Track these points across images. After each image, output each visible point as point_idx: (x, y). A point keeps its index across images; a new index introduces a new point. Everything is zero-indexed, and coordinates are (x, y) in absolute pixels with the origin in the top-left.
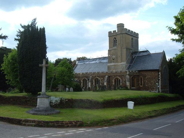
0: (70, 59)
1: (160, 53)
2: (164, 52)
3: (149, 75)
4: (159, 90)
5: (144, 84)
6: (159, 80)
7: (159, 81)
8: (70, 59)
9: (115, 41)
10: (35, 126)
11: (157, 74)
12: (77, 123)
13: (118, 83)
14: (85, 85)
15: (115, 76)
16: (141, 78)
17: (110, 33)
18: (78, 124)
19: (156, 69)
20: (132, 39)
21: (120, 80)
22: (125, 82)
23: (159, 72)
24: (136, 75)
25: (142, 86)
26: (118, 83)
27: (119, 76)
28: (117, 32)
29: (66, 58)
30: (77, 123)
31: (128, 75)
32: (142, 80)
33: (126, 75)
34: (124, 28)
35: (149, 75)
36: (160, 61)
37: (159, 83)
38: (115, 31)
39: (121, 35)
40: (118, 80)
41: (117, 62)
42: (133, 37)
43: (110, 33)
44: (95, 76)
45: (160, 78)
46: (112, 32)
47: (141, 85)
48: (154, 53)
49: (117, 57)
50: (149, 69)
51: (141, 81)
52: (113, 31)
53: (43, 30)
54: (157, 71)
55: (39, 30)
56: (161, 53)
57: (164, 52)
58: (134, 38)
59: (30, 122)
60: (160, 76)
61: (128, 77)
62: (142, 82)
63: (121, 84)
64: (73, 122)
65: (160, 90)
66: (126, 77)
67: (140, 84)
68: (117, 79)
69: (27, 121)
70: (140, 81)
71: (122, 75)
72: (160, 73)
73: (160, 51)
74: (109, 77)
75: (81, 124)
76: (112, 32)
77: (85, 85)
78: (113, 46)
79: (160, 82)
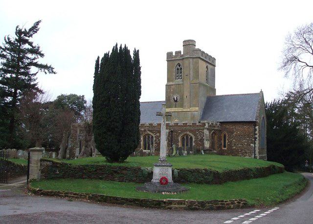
0: (83, 96)
1: (256, 94)
2: (261, 92)
3: (238, 130)
4: (255, 155)
5: (230, 146)
6: (255, 138)
7: (255, 140)
8: (83, 96)
9: (178, 69)
10: (185, 209)
11: (252, 129)
12: (240, 203)
13: (187, 142)
14: (187, 145)
15: (182, 131)
16: (225, 136)
17: (169, 55)
18: (241, 205)
19: (250, 120)
20: (207, 67)
21: (191, 138)
22: (202, 140)
23: (255, 126)
24: (217, 130)
25: (226, 149)
26: (187, 142)
27: (191, 131)
28: (182, 54)
29: (75, 95)
30: (240, 203)
31: (208, 129)
32: (227, 138)
33: (203, 130)
34: (196, 47)
35: (238, 130)
36: (256, 107)
37: (255, 144)
38: (180, 52)
39: (191, 60)
40: (187, 137)
41: (182, 106)
42: (208, 65)
43: (169, 55)
44: (145, 131)
45: (257, 136)
46: (174, 54)
47: (225, 147)
48: (246, 94)
49: (182, 98)
50: (239, 120)
51: (225, 141)
52: (176, 53)
53: (115, 50)
54: (253, 123)
55: (118, 50)
56: (258, 94)
57: (261, 92)
58: (210, 67)
59: (175, 204)
60: (257, 132)
61: (206, 132)
62: (227, 141)
63: (194, 144)
64: (236, 202)
65: (257, 155)
66: (203, 133)
67: (223, 144)
68: (187, 136)
69: (170, 203)
70: (223, 139)
71: (196, 129)
72: (257, 127)
73: (258, 91)
74: (172, 131)
75: (244, 204)
76: (174, 54)
77: (187, 145)
78: (176, 79)
79: (257, 142)
